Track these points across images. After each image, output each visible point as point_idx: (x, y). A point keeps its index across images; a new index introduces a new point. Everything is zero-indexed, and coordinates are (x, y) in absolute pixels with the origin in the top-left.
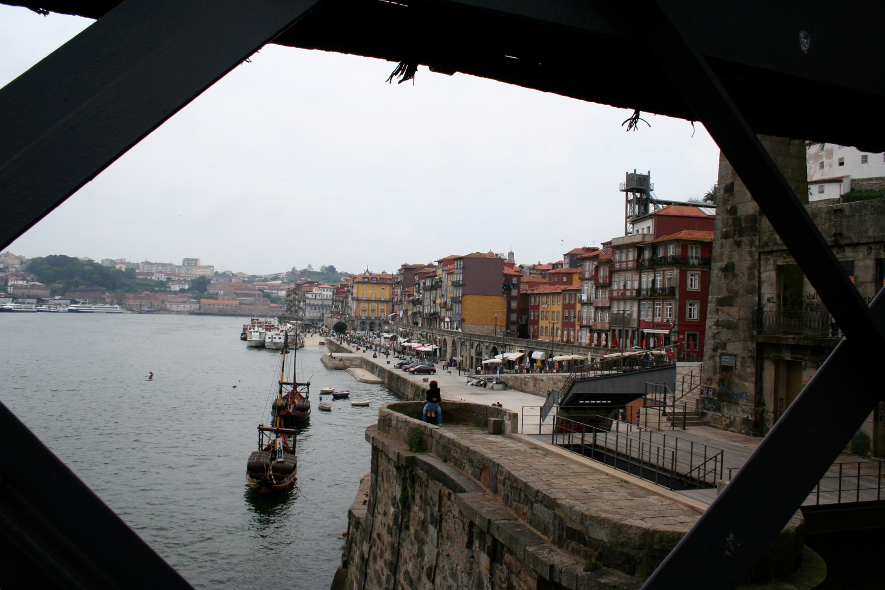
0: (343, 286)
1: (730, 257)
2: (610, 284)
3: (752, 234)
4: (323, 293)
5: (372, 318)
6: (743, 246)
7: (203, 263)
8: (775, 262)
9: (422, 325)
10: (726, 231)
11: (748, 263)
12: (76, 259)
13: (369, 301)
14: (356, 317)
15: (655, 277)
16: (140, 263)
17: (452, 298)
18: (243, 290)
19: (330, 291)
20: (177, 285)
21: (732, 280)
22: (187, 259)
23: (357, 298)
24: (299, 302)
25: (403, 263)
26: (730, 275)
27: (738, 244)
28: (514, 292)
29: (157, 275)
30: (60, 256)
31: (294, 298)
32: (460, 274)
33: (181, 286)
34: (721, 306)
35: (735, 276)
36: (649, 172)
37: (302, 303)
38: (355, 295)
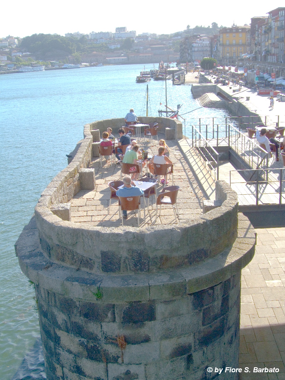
0: (216, 37)
4: (203, 42)
5: (234, 58)
7: (129, 30)
9: (261, 60)
12: (49, 35)
13: (231, 45)
14: (223, 58)
16: (88, 34)
17: (278, 39)
18: (155, 45)
19: (208, 41)
20: (113, 46)
22: (118, 28)
23: (223, 44)
24: (188, 50)
25: (252, 17)
29: (100, 40)
30: (40, 34)
31: (185, 48)
32: (282, 20)
33: (115, 46)
37: (190, 51)
38: (221, 42)
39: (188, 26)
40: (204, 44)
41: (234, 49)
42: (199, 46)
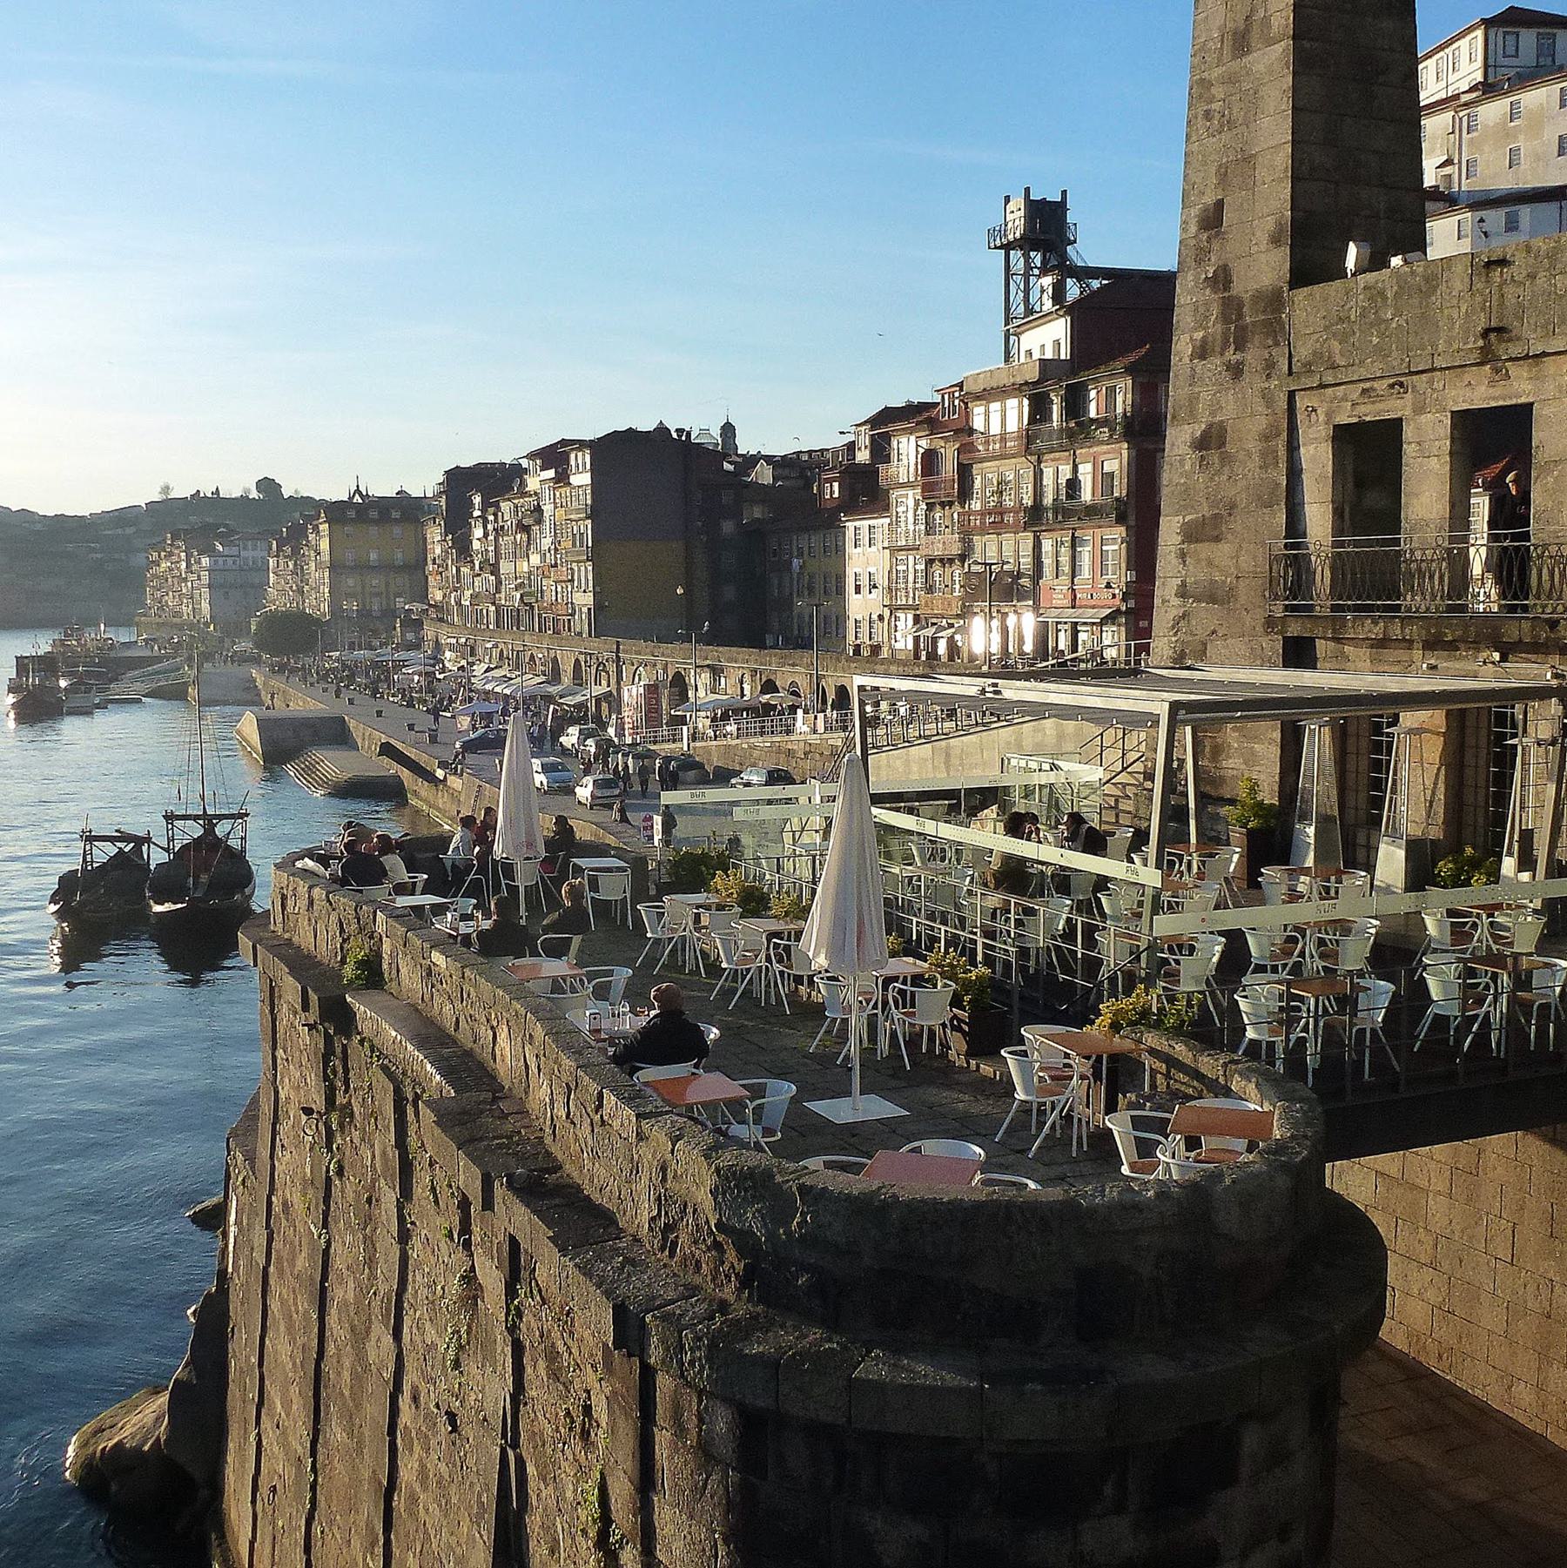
1: (1216, 408)
2: (965, 493)
3: (1271, 343)
6: (1246, 376)
8: (1329, 415)
10: (1204, 340)
11: (1261, 423)
15: (1075, 469)
21: (1218, 473)
26: (1214, 457)
27: (1236, 371)
28: (728, 527)
34: (1190, 542)
35: (1226, 459)
36: (1064, 193)
39: (166, 489)
40: (247, 558)
41: (374, 582)
42: (226, 567)
